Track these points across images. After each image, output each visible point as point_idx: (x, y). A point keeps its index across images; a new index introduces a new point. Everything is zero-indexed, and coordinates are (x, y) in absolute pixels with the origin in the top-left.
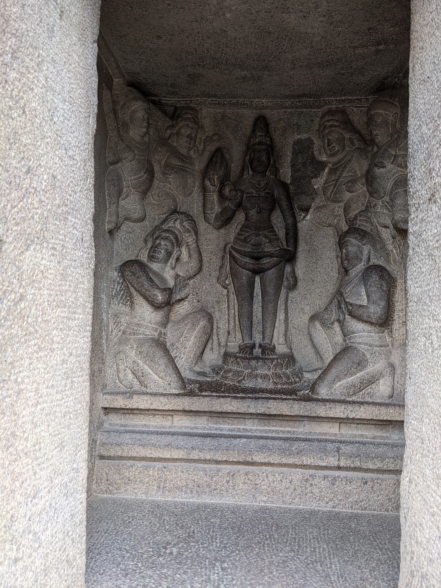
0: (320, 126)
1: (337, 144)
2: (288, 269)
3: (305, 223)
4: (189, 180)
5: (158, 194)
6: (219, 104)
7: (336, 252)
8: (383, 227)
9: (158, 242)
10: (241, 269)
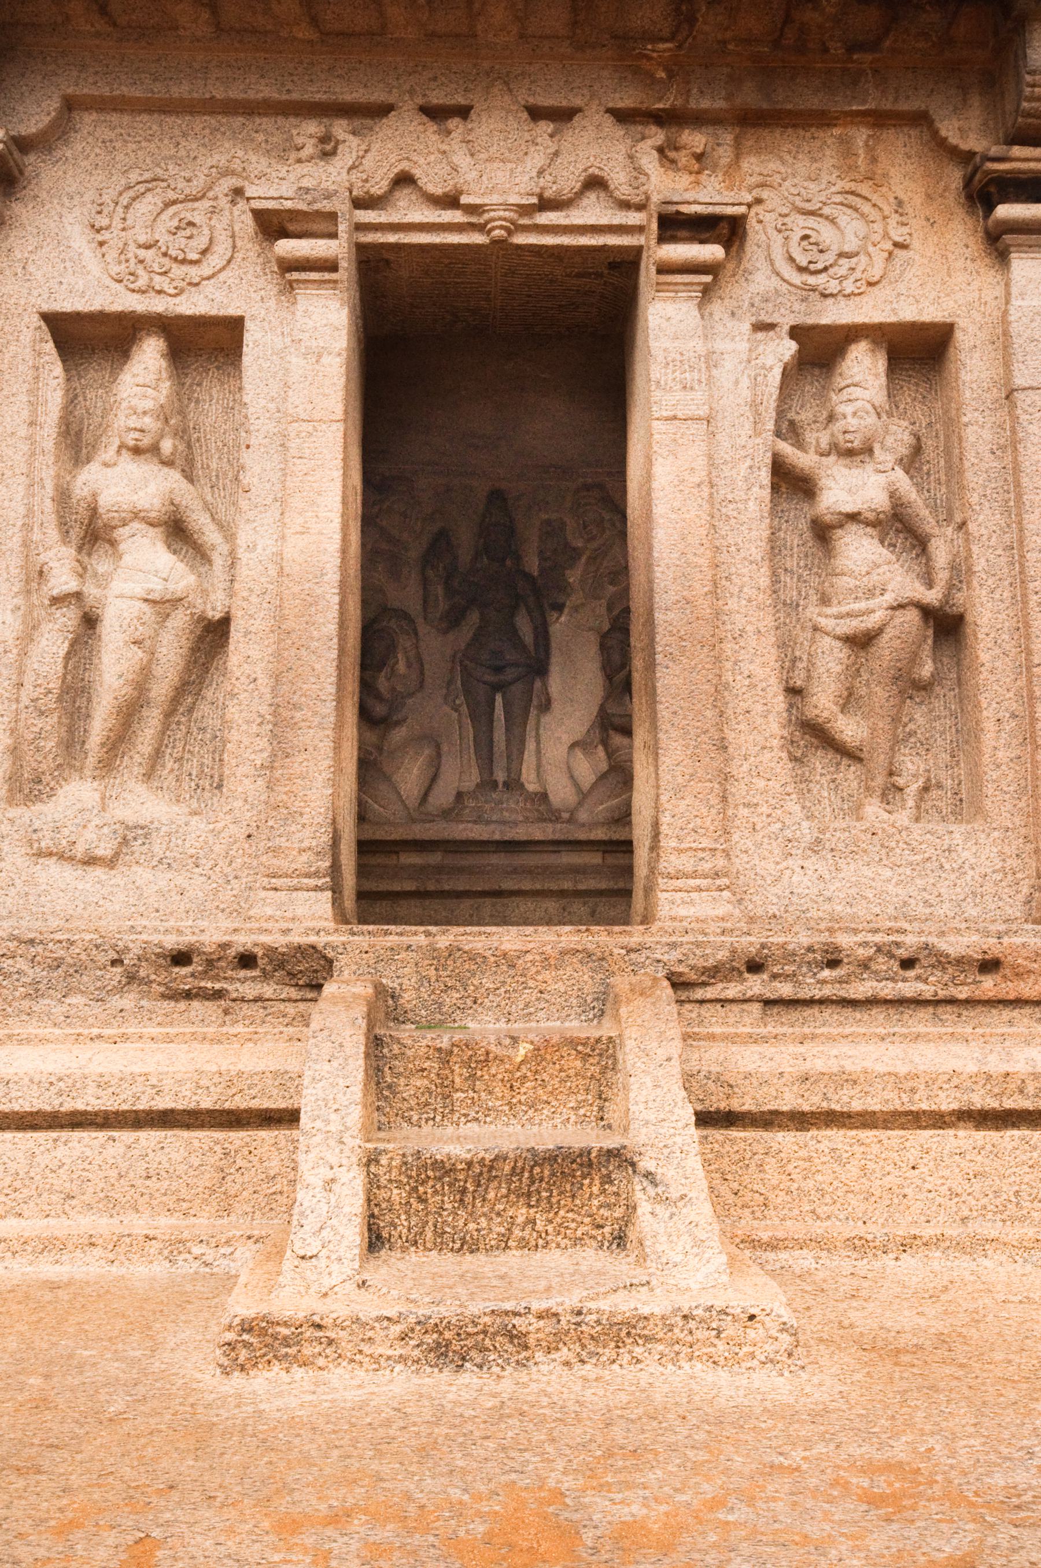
3: (560, 625)
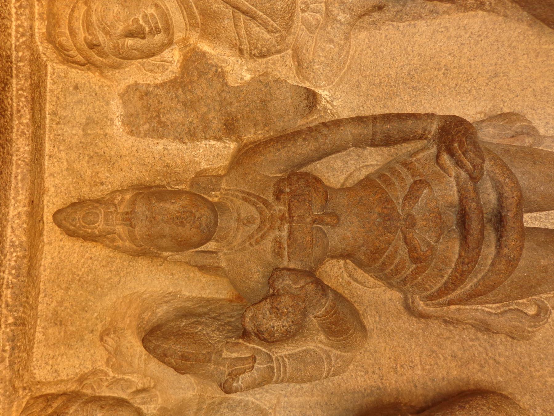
2: (487, 135)
3: (338, 101)
7: (420, 17)
10: (517, 273)
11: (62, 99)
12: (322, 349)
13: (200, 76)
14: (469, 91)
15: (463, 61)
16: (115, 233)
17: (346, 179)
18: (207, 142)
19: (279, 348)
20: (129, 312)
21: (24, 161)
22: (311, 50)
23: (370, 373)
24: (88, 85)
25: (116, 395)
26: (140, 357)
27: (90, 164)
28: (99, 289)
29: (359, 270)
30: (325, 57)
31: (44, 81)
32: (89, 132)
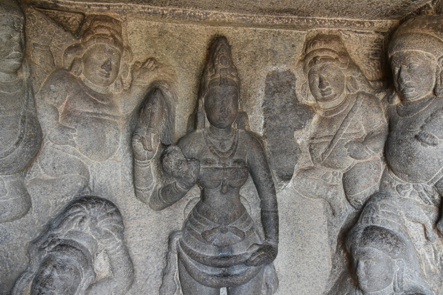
0: (306, 56)
1: (334, 86)
2: (268, 271)
3: (286, 193)
4: (107, 136)
5: (53, 164)
6: (155, 13)
7: (330, 235)
8: (413, 221)
9: (47, 272)
11: (287, 38)
12: (153, 186)
13: (300, 115)
14: (290, 263)
15: (306, 259)
16: (215, 73)
17: (243, 198)
18: (263, 119)
19: (155, 163)
20: (167, 75)
21: (253, 20)
22: (313, 177)
23: (137, 213)
24: (295, 52)
25: (120, 68)
26: (143, 83)
27: (251, 52)
28: (179, 57)
29: (194, 205)
30: (309, 185)
31: (296, 29)
32: (269, 53)
